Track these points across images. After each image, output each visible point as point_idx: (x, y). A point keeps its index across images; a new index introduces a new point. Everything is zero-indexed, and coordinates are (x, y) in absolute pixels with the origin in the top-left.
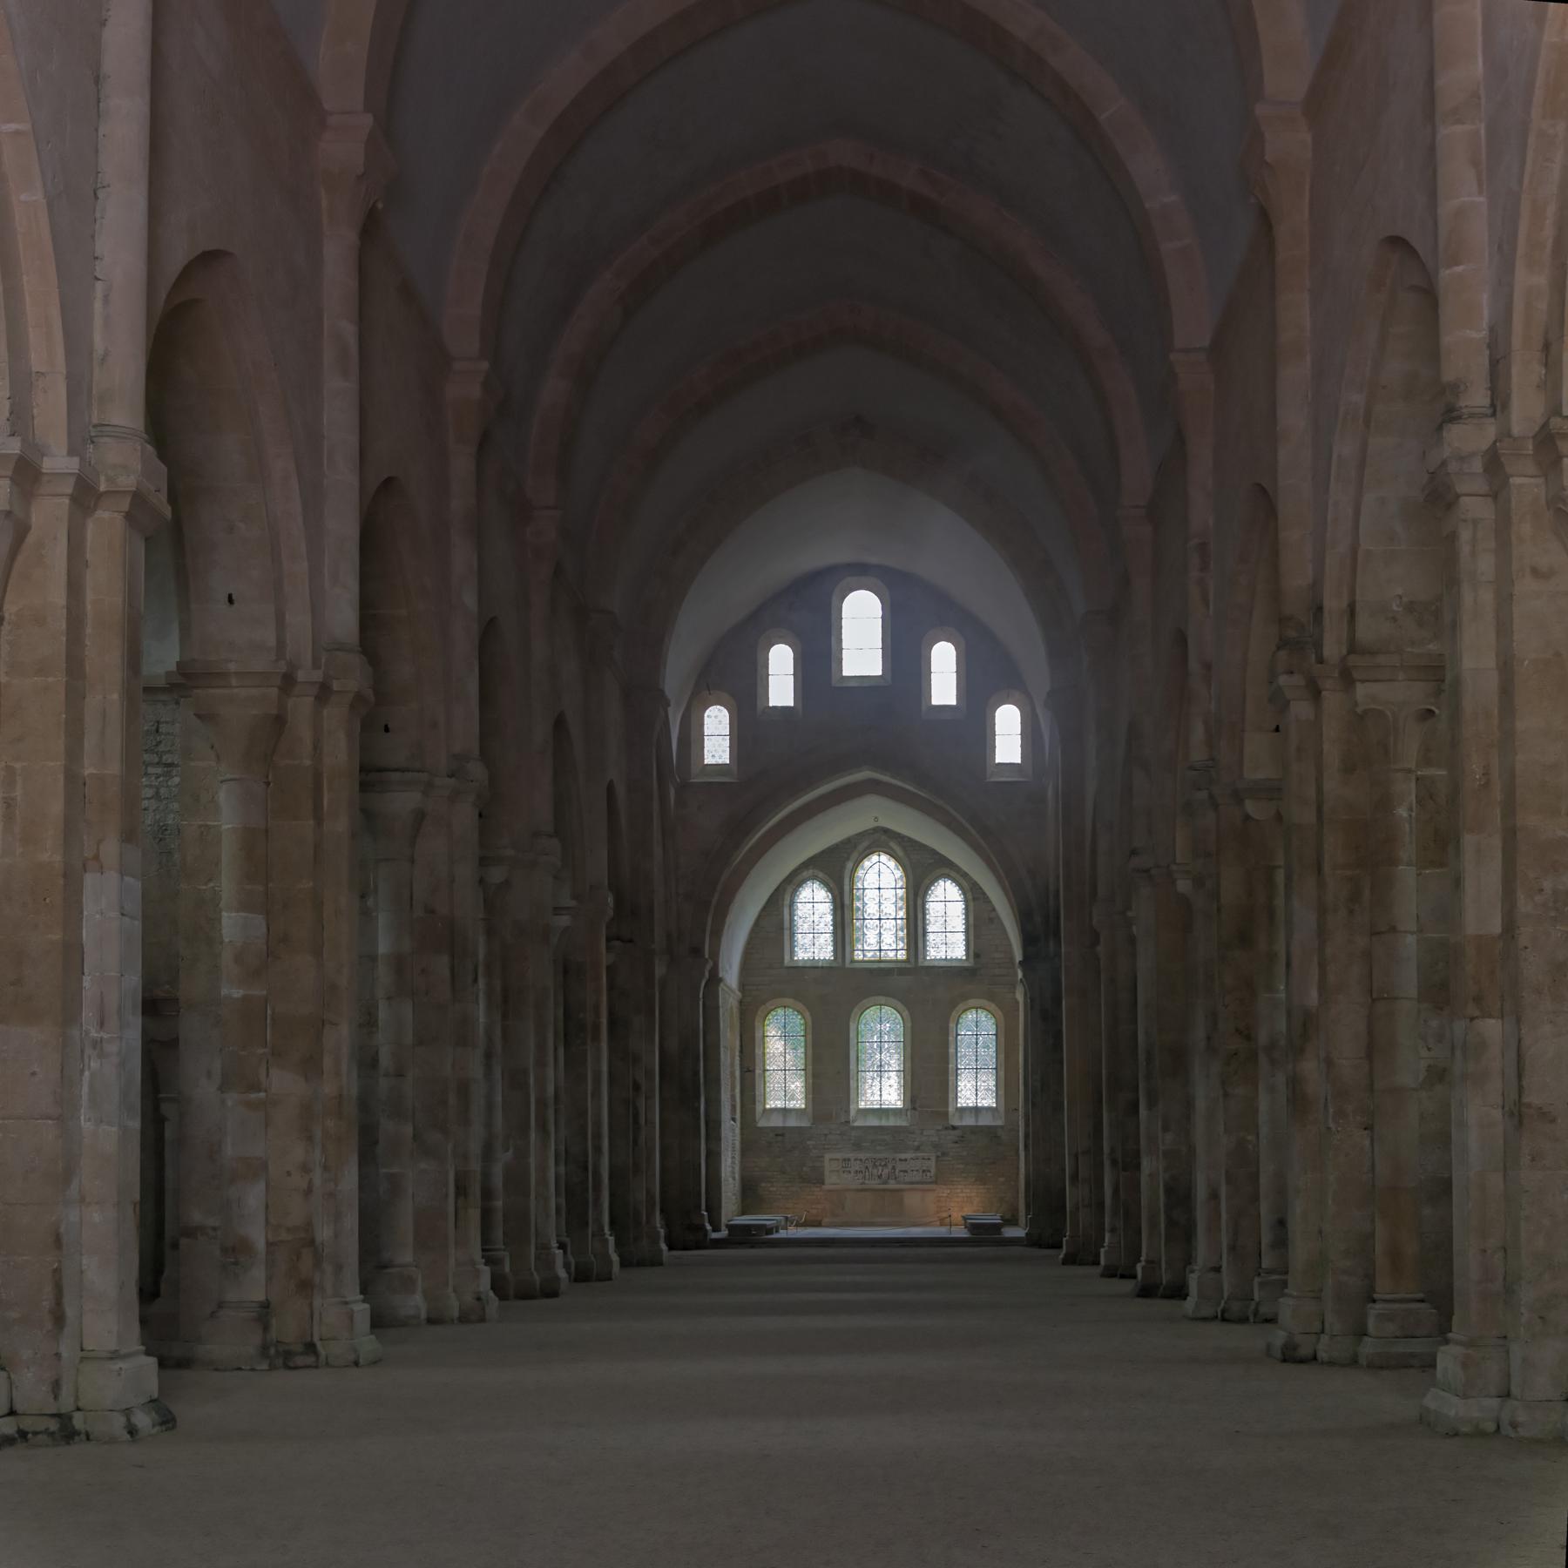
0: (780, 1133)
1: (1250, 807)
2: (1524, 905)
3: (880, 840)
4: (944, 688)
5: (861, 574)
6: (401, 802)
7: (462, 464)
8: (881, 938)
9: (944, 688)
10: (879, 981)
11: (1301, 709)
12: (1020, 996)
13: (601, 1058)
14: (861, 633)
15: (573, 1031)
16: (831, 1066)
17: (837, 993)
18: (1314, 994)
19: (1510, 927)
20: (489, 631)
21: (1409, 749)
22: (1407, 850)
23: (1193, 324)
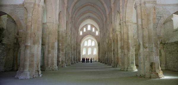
0: (84, 55)
1: (111, 38)
3: (90, 39)
4: (94, 30)
5: (89, 24)
6: (67, 37)
7: (70, 20)
8: (89, 44)
9: (94, 30)
10: (90, 47)
11: (113, 34)
12: (97, 48)
13: (75, 51)
14: (89, 28)
15: (74, 50)
16: (87, 52)
17: (87, 48)
19: (124, 45)
20: (71, 28)
22: (119, 41)
23: (107, 13)
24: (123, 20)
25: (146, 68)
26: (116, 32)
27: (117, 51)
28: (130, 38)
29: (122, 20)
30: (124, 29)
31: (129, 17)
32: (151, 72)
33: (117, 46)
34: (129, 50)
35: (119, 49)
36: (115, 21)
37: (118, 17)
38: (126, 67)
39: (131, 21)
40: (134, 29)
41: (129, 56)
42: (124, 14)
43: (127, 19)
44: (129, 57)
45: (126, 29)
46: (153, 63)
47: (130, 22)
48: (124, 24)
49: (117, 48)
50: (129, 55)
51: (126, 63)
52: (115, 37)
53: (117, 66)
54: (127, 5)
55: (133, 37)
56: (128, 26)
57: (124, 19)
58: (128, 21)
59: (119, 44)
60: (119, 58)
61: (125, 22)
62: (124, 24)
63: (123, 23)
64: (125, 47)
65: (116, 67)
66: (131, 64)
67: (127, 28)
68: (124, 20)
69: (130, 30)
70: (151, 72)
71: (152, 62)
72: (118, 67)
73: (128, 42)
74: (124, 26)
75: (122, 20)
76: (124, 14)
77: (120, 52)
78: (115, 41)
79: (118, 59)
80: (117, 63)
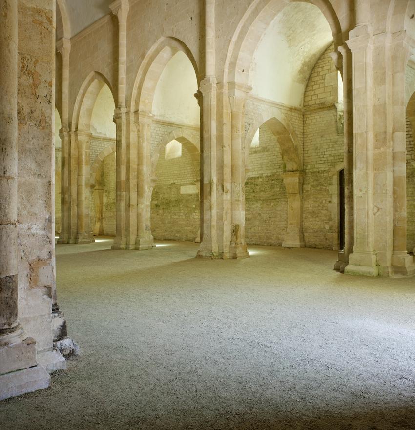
2: (131, 177)
18: (68, 184)
21: (84, 147)
24: (128, 105)
25: (224, 237)
26: (76, 135)
27: (79, 193)
28: (145, 161)
29: (124, 104)
30: (132, 133)
31: (147, 101)
32: (234, 245)
33: (78, 180)
34: (140, 194)
35: (84, 187)
36: (78, 98)
37: (90, 89)
38: (133, 238)
39: (151, 115)
41: (142, 210)
42: (135, 91)
43: (141, 107)
44: (140, 211)
45: (136, 133)
46: (239, 225)
47: (150, 117)
48: (132, 118)
49: (79, 186)
50: (142, 207)
51: (133, 229)
52: (72, 151)
53: (76, 239)
54: (150, 69)
55: (151, 158)
56: (143, 126)
57: (133, 104)
58: (143, 111)
59: (84, 174)
60: (84, 215)
61: (136, 112)
62: (132, 118)
63: (128, 113)
64: (132, 185)
65: (76, 243)
66: (145, 231)
67: (139, 131)
68: (133, 109)
69: (145, 137)
70: (234, 245)
71: (238, 223)
72: (81, 243)
73: (138, 169)
74: (132, 125)
75: (124, 104)
76: (135, 91)
77: (86, 198)
78: (73, 161)
79: (79, 216)
80: (77, 229)
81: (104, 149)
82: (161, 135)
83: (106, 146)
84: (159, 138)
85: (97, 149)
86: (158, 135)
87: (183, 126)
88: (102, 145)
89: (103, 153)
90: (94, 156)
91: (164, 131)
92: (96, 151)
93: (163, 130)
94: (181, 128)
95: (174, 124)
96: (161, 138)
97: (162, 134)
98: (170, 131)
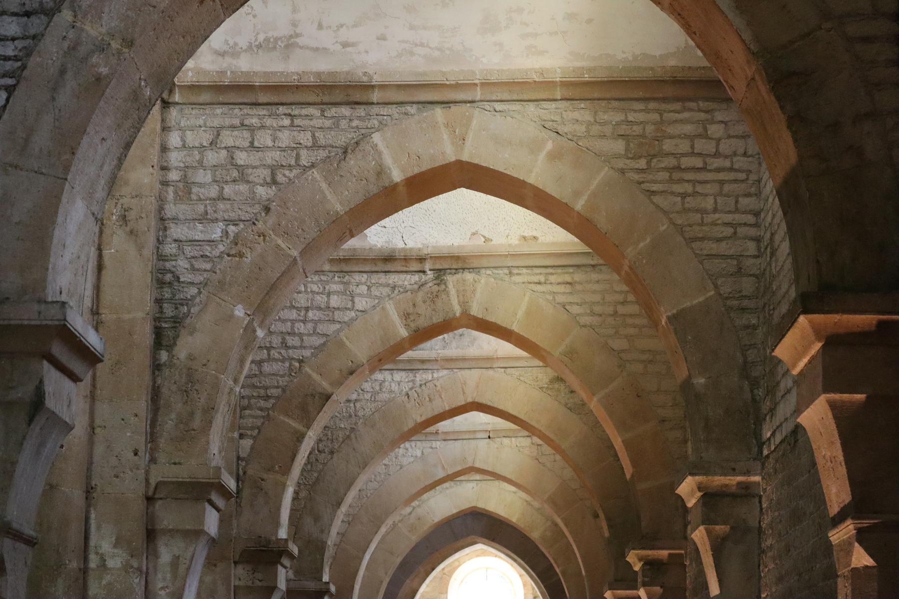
40: (186, 187)
81: (349, 324)
82: (266, 173)
83: (361, 303)
84: (252, 198)
85: (301, 328)
86: (243, 178)
87: (457, 86)
88: (335, 301)
89: (341, 345)
90: (276, 367)
91: (297, 147)
92: (291, 341)
93: (285, 138)
94: (446, 103)
95: (370, 87)
96: (262, 192)
97: (274, 169)
98: (342, 139)
